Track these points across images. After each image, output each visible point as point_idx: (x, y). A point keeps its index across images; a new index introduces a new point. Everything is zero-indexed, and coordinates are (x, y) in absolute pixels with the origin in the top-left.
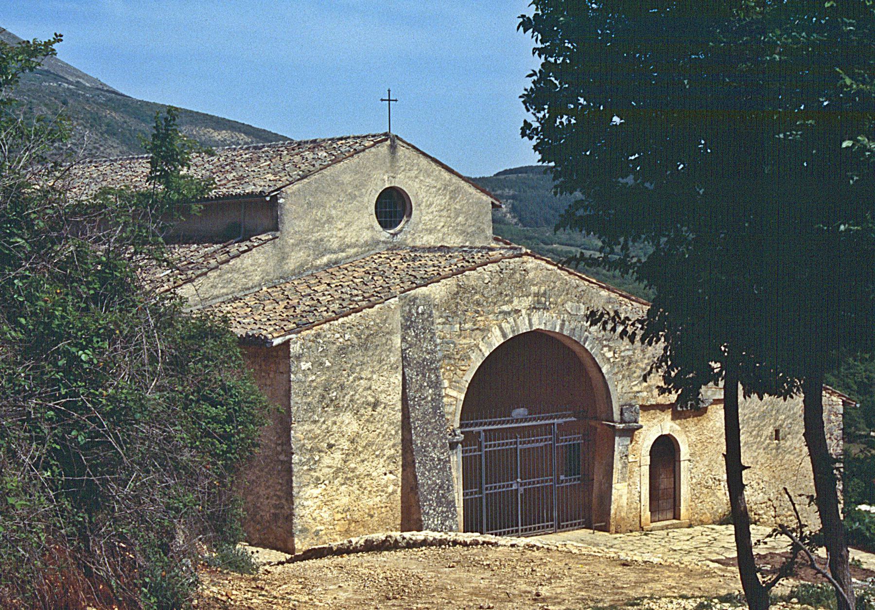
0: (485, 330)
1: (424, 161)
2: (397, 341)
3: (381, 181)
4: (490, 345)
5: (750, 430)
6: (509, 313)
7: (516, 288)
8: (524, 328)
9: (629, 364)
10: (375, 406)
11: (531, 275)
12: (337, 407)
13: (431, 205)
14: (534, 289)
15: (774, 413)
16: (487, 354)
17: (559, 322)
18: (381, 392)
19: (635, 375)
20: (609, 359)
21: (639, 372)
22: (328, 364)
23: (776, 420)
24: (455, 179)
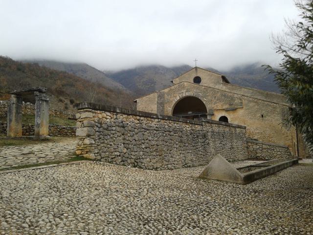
0: (176, 97)
3: (194, 75)
8: (184, 95)
23: (261, 112)
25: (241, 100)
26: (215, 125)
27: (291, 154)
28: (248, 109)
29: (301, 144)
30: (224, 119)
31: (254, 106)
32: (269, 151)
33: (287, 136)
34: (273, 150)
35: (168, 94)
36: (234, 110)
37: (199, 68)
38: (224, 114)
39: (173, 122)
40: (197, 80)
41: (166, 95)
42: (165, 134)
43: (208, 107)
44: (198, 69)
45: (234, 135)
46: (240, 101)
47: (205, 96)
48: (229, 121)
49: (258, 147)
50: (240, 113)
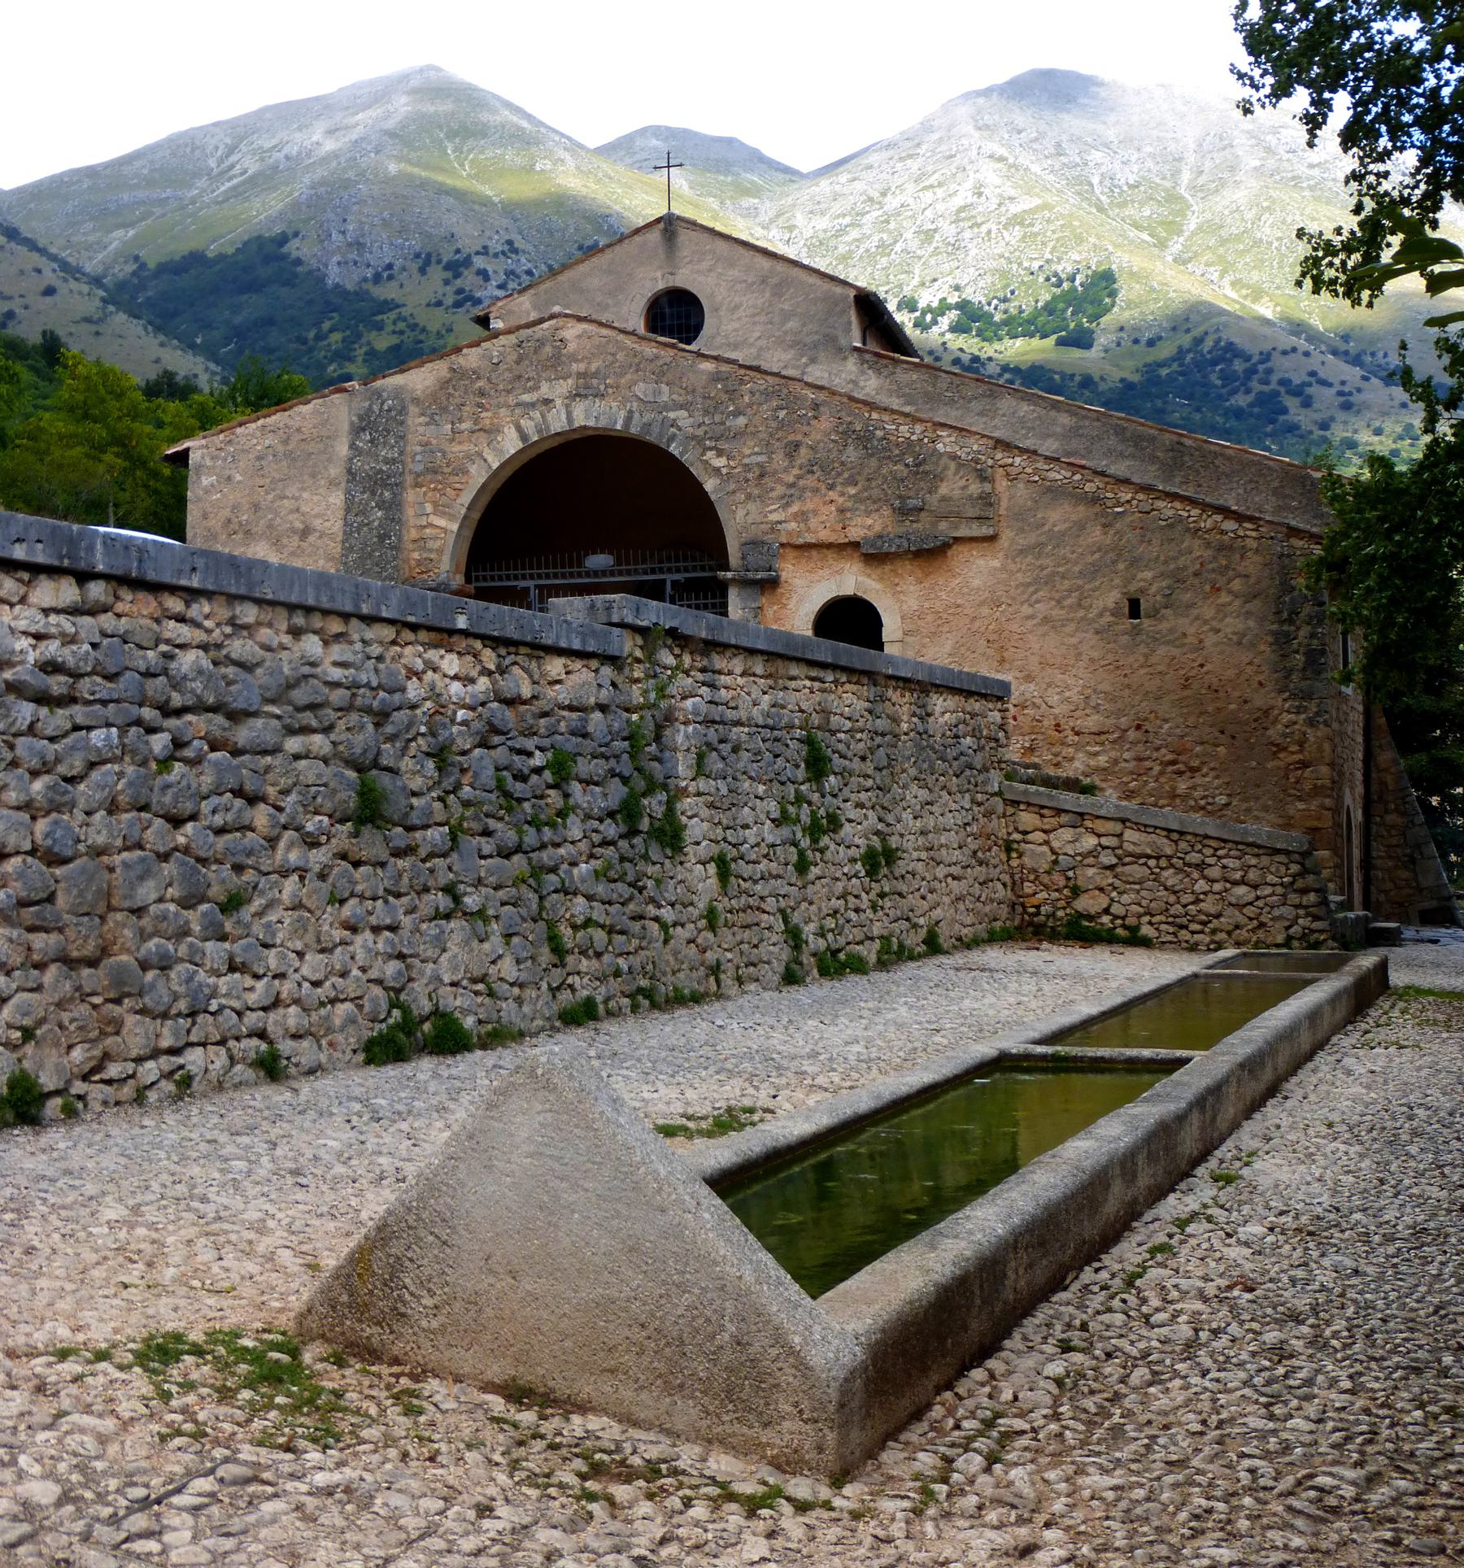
0: (492, 431)
1: (721, 245)
2: (343, 449)
3: (653, 281)
4: (499, 452)
5: (1057, 596)
6: (533, 405)
7: (546, 368)
8: (558, 422)
9: (762, 476)
10: (305, 533)
11: (572, 347)
12: (248, 532)
13: (737, 307)
14: (582, 367)
15: (1121, 566)
16: (495, 465)
17: (623, 414)
18: (317, 516)
19: (773, 494)
20: (717, 470)
21: (780, 490)
22: (238, 478)
23: (1127, 582)
24: (780, 267)
25: (983, 477)
26: (737, 664)
27: (1325, 902)
28: (1037, 549)
29: (1391, 818)
30: (850, 621)
31: (1081, 526)
32: (1170, 877)
33: (1304, 765)
34: (1201, 866)
35: (438, 405)
36: (930, 554)
37: (693, 224)
38: (850, 579)
39: (282, 621)
40: (676, 315)
41: (415, 420)
42: (159, 743)
43: (739, 520)
44: (684, 236)
45: (906, 746)
46: (975, 488)
47: (720, 439)
48: (887, 634)
49: (1090, 842)
50: (976, 583)
